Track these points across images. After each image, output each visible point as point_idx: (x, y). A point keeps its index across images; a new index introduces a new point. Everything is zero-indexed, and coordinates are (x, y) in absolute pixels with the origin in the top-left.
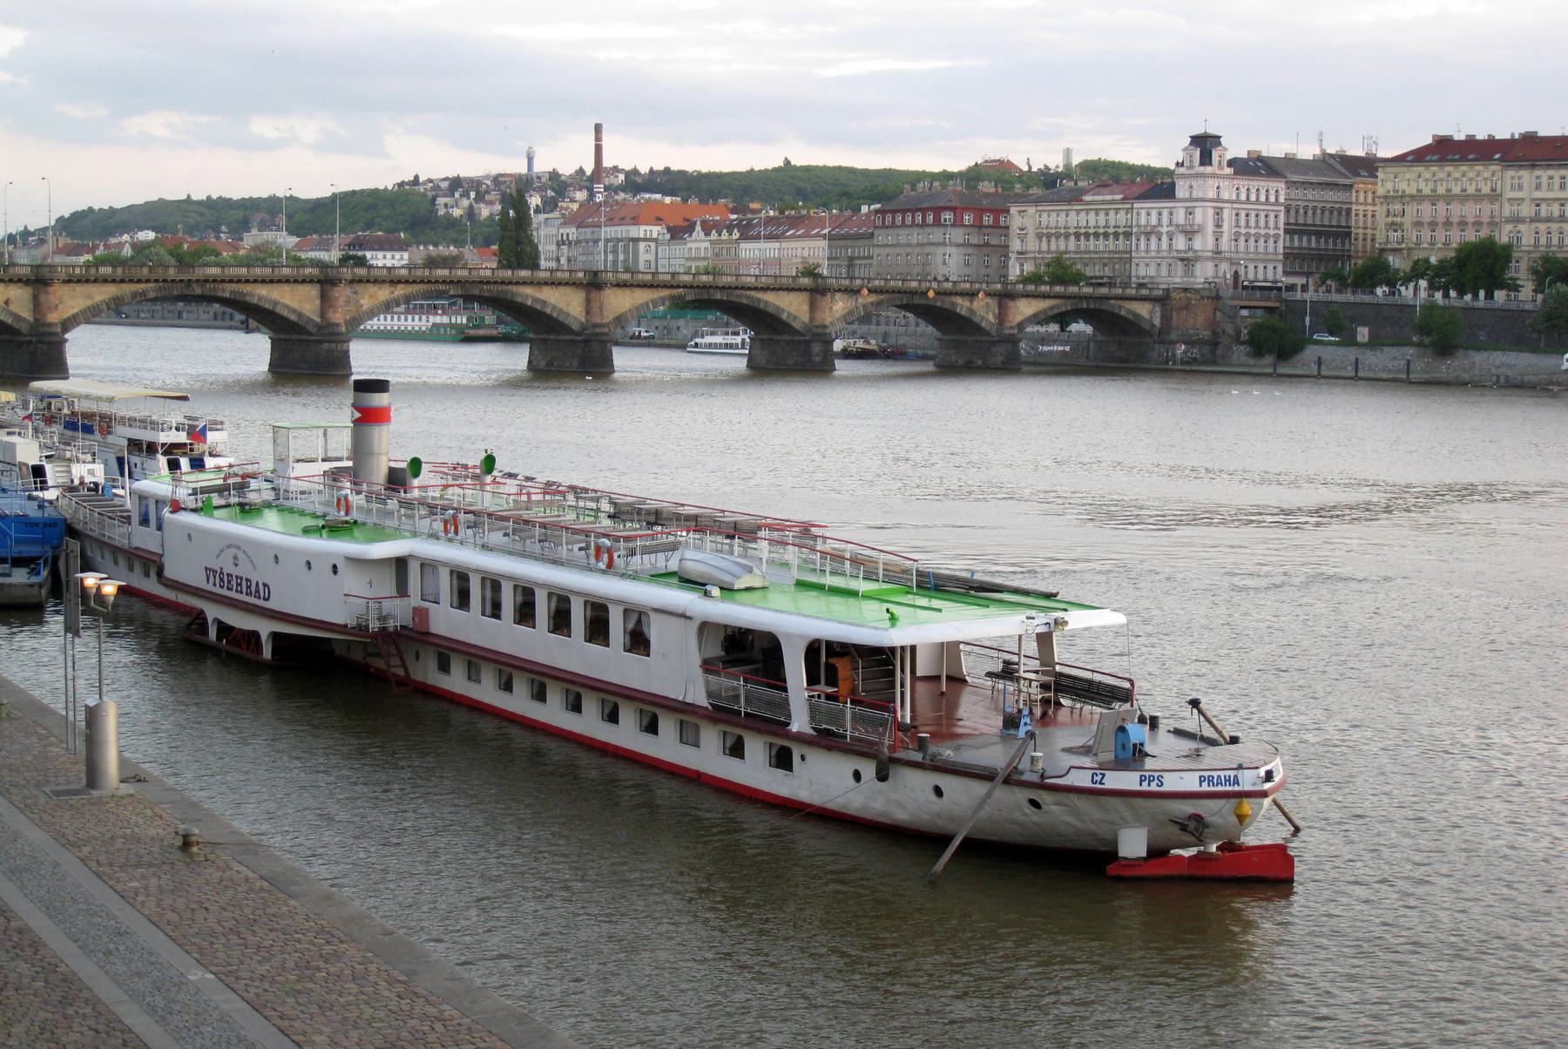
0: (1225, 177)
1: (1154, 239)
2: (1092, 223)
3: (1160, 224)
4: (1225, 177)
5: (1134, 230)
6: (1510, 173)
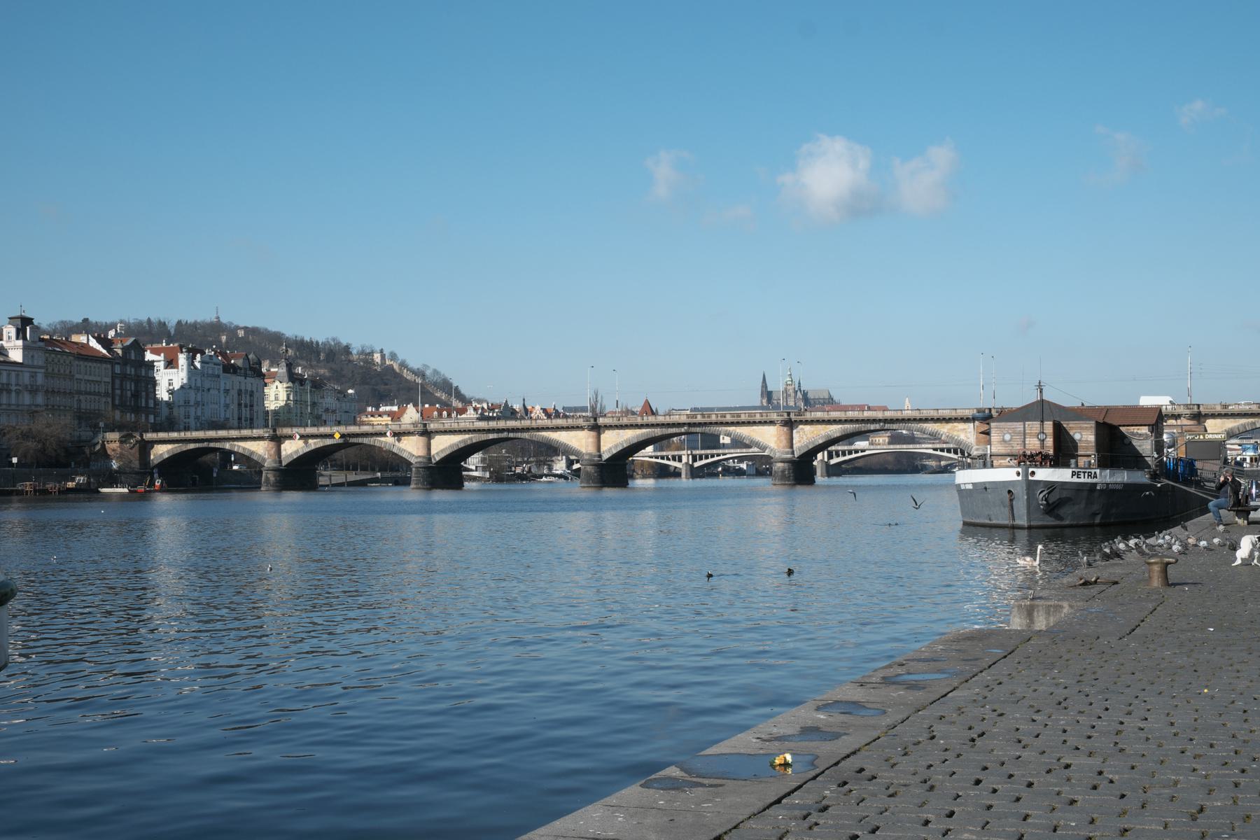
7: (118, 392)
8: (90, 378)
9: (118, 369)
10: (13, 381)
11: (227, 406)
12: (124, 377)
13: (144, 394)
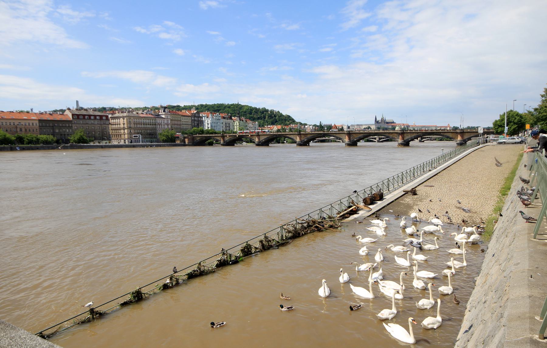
0: (169, 114)
1: (161, 125)
2: (116, 122)
3: (162, 123)
4: (169, 114)
5: (157, 124)
6: (182, 117)
7: (193, 124)
8: (185, 121)
9: (193, 118)
10: (163, 122)
11: (222, 127)
12: (195, 120)
13: (200, 124)
